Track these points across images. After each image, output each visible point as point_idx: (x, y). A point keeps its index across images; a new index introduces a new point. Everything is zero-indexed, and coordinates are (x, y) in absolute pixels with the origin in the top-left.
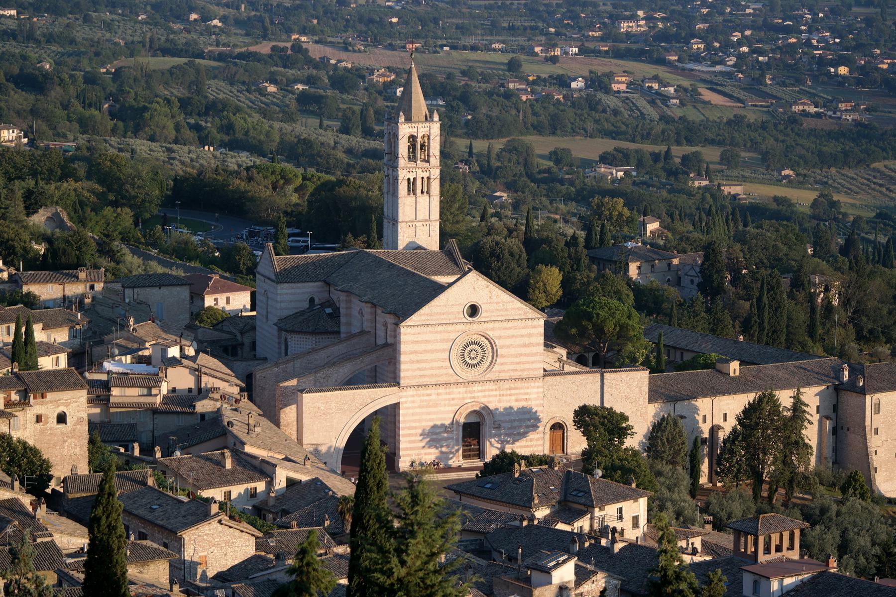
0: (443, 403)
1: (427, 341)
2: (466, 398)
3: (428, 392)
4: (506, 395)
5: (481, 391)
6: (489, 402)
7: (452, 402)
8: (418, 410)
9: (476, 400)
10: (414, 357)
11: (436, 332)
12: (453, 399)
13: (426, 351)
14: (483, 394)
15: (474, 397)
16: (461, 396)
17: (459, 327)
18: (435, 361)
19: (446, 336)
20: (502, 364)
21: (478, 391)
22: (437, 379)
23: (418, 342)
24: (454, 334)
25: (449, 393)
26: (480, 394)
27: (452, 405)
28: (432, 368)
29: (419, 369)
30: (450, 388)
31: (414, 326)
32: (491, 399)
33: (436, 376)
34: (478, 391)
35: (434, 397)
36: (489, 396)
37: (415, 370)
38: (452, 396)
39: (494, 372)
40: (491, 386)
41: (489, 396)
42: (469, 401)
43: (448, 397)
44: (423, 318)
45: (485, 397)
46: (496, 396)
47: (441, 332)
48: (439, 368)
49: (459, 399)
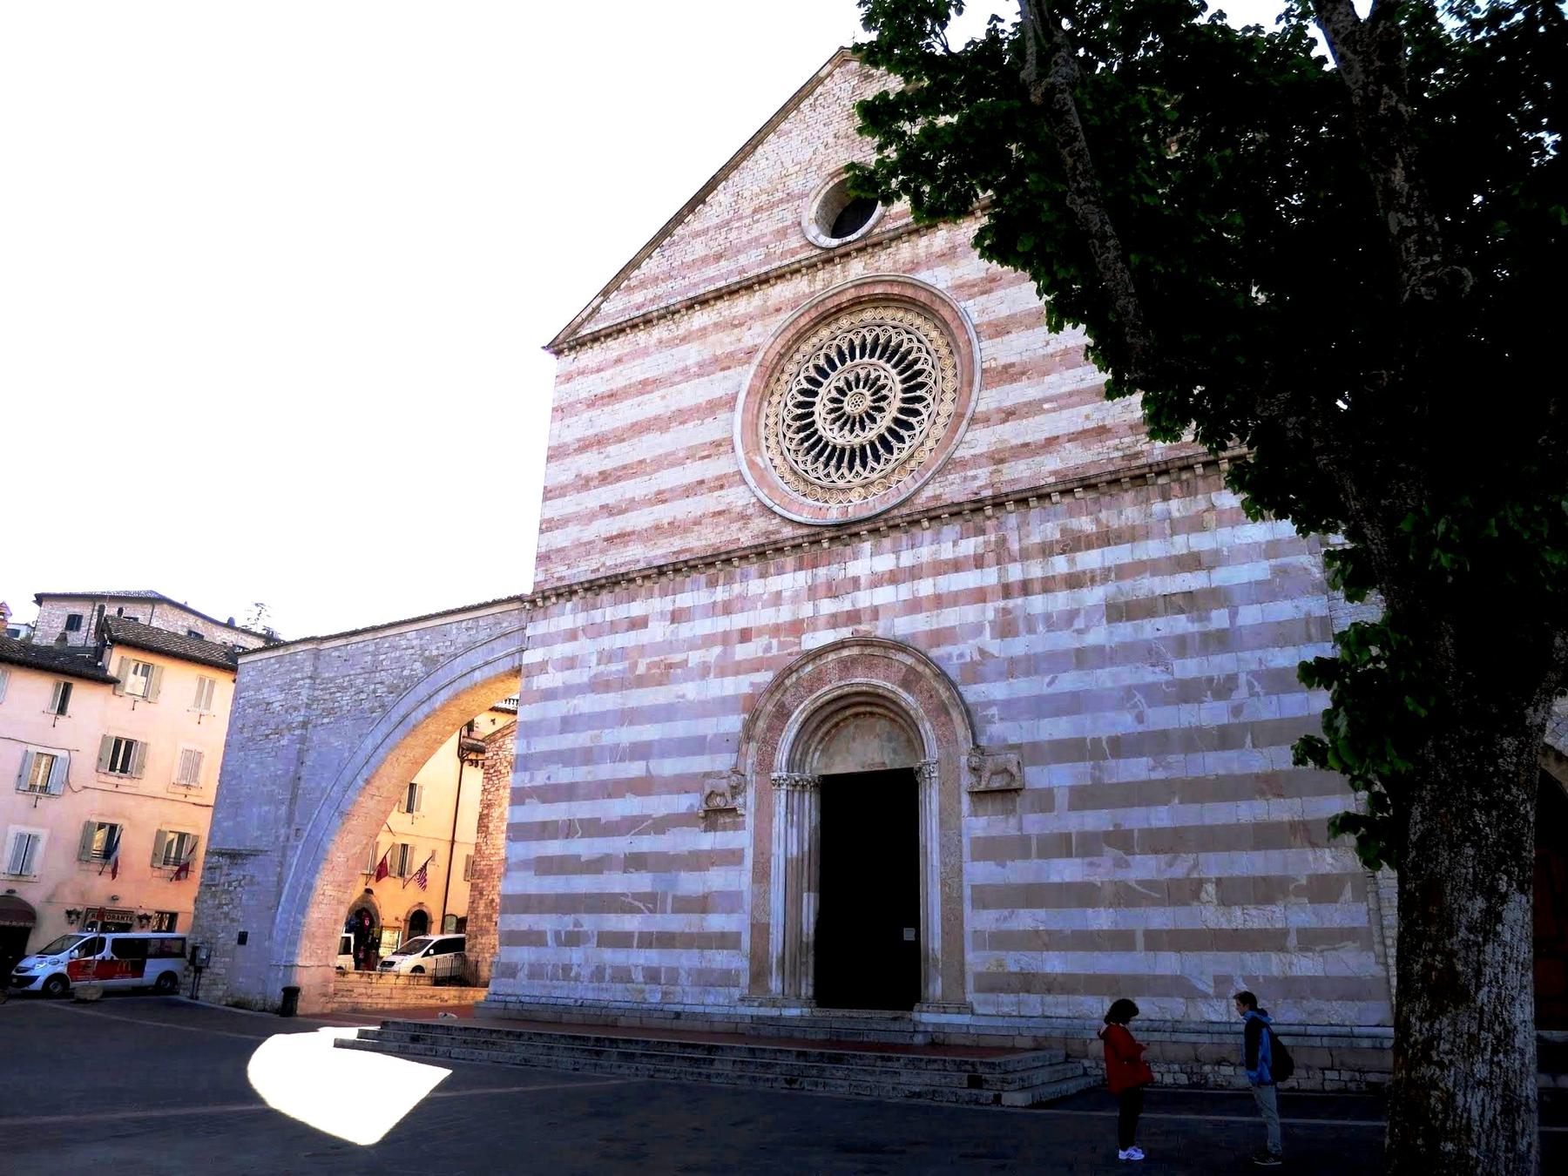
0: (695, 658)
1: (645, 386)
2: (812, 624)
3: (636, 609)
4: (1048, 585)
5: (894, 578)
6: (940, 636)
7: (742, 652)
8: (587, 704)
9: (864, 627)
10: (591, 463)
11: (684, 339)
12: (745, 635)
13: (639, 428)
14: (904, 591)
15: (853, 617)
16: (785, 615)
17: (780, 292)
18: (672, 465)
19: (725, 343)
20: (1009, 414)
21: (877, 581)
22: (677, 543)
23: (612, 396)
24: (758, 327)
25: (727, 609)
26: (885, 595)
27: (739, 669)
28: (660, 498)
29: (609, 510)
30: (730, 581)
31: (595, 338)
32: (950, 617)
33: (674, 528)
34: (877, 581)
35: (658, 631)
36: (939, 601)
37: (592, 517)
38: (739, 621)
39: (963, 464)
40: (952, 544)
41: (939, 601)
42: (826, 637)
43: (722, 624)
44: (638, 297)
45: (914, 606)
46: (980, 595)
47: (703, 332)
48: (689, 491)
49: (776, 630)
